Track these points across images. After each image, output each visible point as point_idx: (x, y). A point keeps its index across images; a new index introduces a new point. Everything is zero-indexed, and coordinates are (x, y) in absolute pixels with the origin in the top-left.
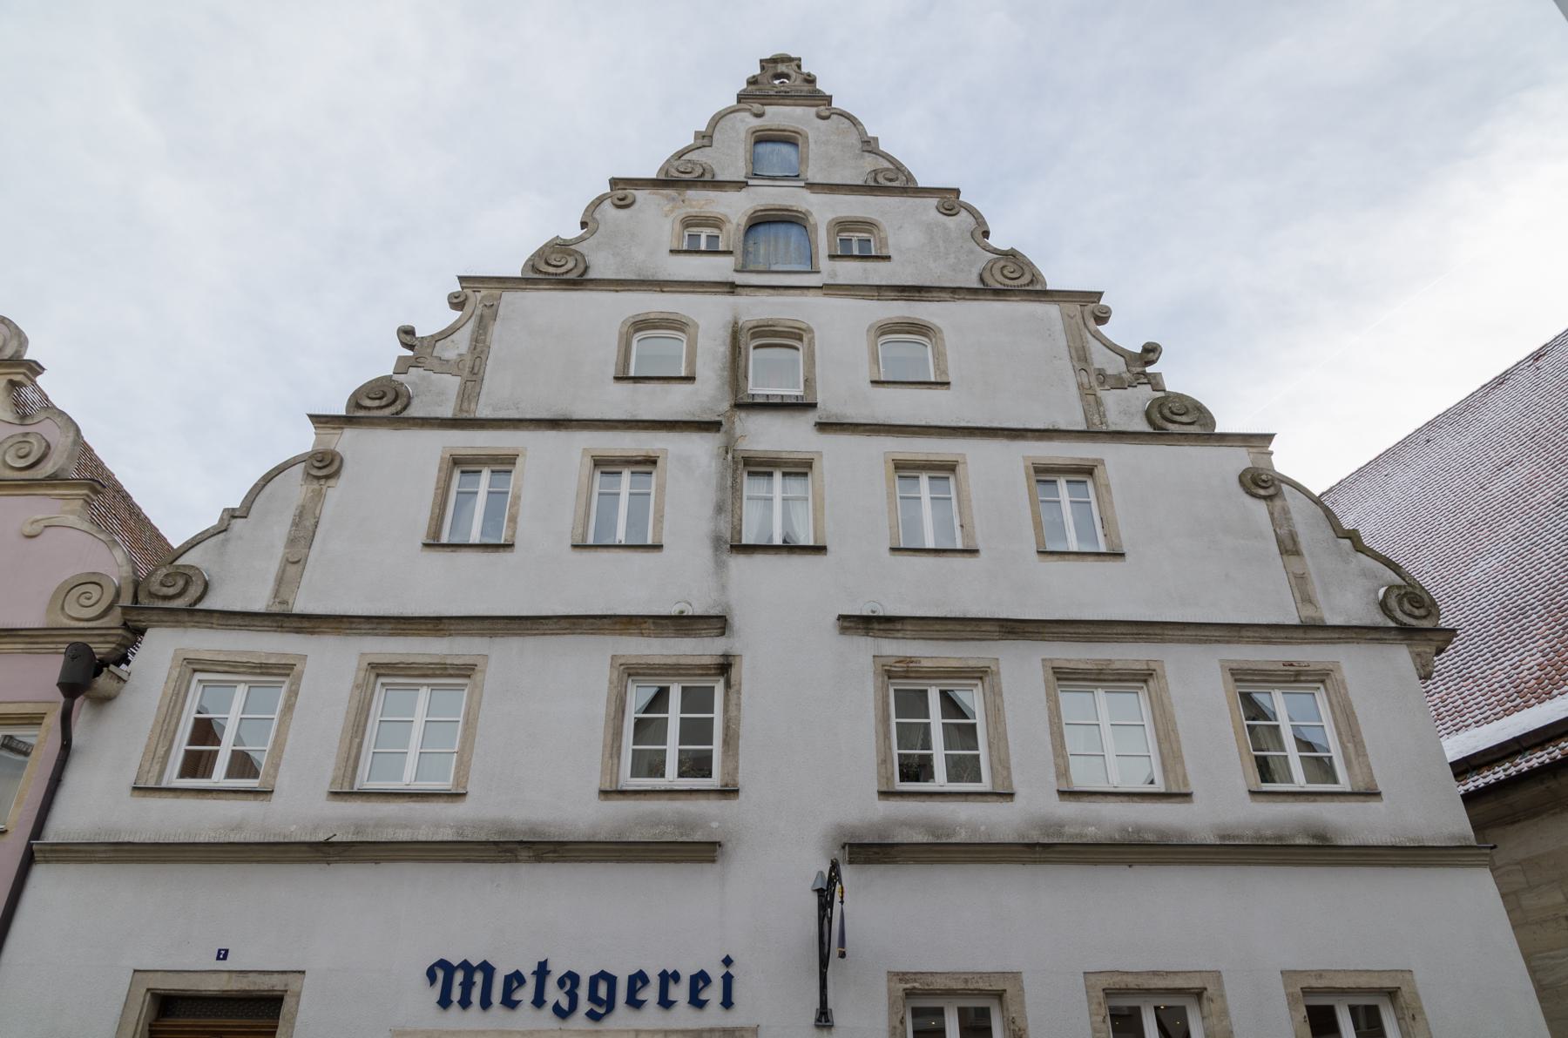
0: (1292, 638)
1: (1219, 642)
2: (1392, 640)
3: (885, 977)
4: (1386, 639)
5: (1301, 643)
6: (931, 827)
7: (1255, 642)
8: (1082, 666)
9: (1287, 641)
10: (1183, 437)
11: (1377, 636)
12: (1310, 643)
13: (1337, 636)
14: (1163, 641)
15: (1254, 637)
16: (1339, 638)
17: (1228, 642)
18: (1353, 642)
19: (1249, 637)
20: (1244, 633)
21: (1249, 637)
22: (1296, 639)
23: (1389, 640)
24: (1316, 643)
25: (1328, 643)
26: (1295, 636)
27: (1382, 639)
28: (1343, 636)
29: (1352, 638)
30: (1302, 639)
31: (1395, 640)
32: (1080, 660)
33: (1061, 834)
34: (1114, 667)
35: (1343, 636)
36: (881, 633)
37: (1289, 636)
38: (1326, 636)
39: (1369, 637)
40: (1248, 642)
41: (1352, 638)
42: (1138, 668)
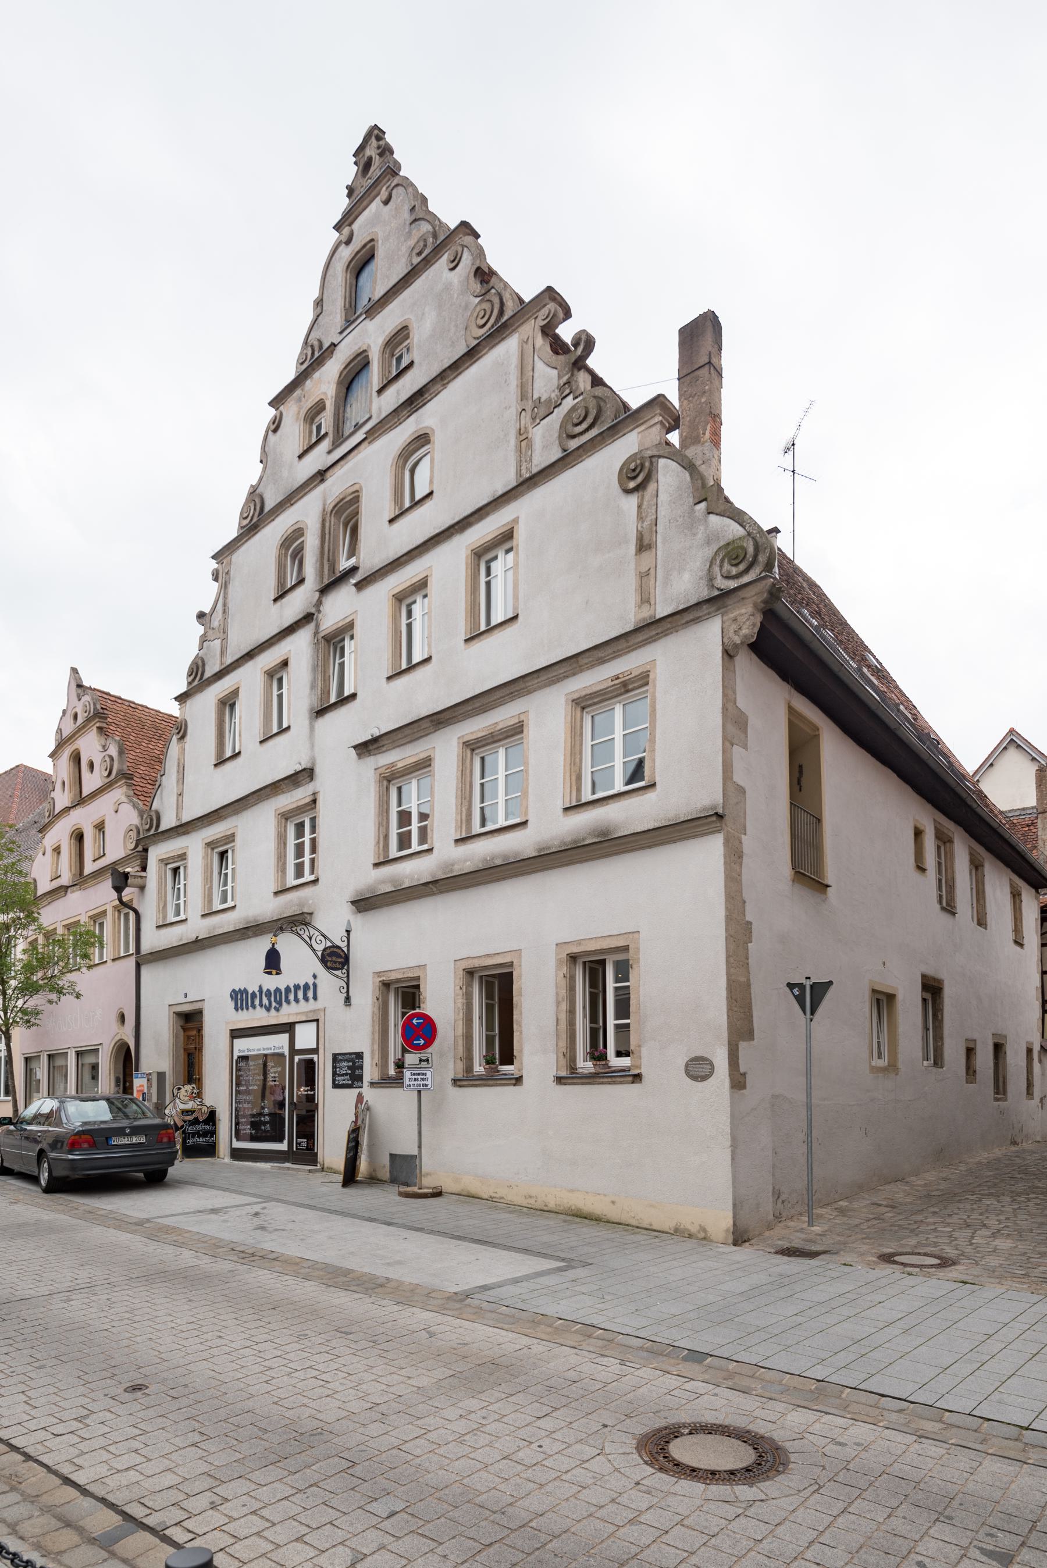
0: (618, 651)
1: (567, 677)
2: (706, 615)
3: (371, 974)
4: (700, 617)
5: (629, 652)
6: (393, 881)
7: (593, 666)
8: (480, 735)
9: (616, 656)
10: (581, 450)
11: (691, 617)
12: (636, 649)
13: (654, 633)
14: (529, 692)
15: (591, 662)
16: (657, 634)
17: (574, 674)
18: (672, 633)
19: (586, 664)
20: (583, 661)
21: (586, 664)
22: (622, 650)
23: (704, 616)
24: (640, 647)
25: (650, 642)
26: (620, 647)
27: (698, 618)
28: (659, 631)
29: (669, 629)
30: (627, 648)
31: (709, 613)
32: (479, 730)
33: (452, 871)
34: (499, 728)
35: (659, 631)
36: (376, 752)
37: (615, 650)
38: (645, 637)
39: (683, 621)
40: (588, 669)
41: (669, 629)
42: (512, 723)
